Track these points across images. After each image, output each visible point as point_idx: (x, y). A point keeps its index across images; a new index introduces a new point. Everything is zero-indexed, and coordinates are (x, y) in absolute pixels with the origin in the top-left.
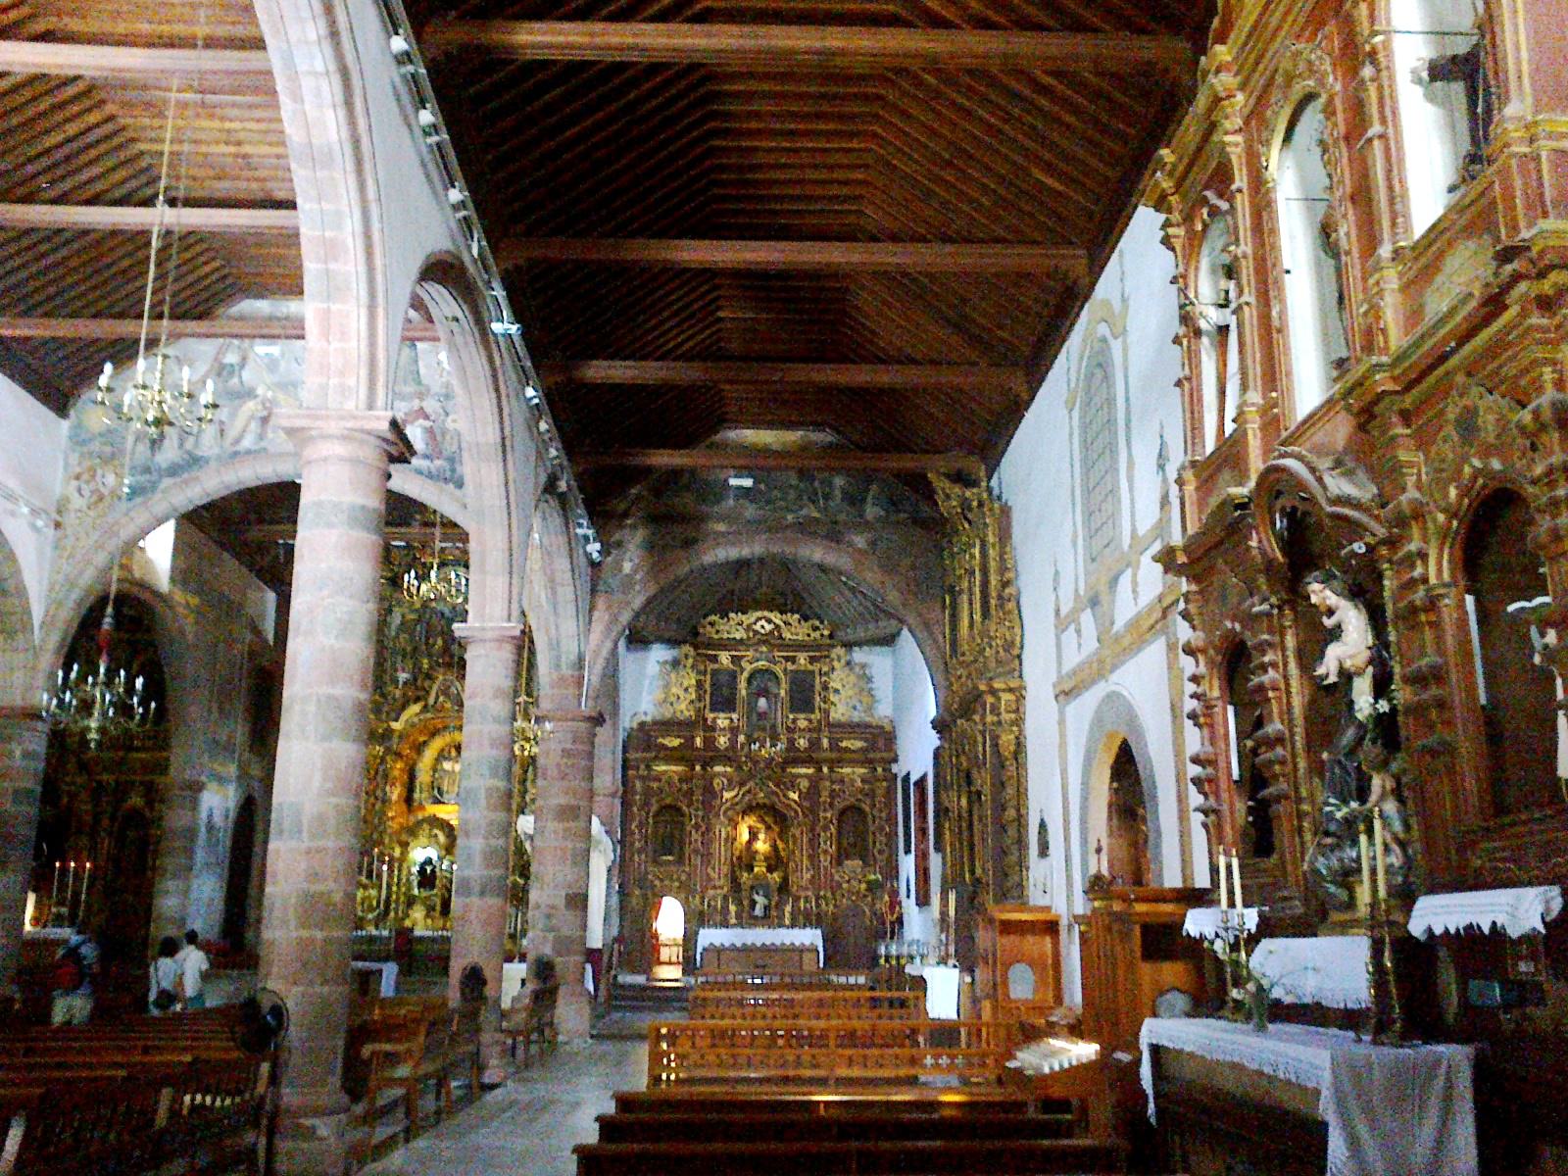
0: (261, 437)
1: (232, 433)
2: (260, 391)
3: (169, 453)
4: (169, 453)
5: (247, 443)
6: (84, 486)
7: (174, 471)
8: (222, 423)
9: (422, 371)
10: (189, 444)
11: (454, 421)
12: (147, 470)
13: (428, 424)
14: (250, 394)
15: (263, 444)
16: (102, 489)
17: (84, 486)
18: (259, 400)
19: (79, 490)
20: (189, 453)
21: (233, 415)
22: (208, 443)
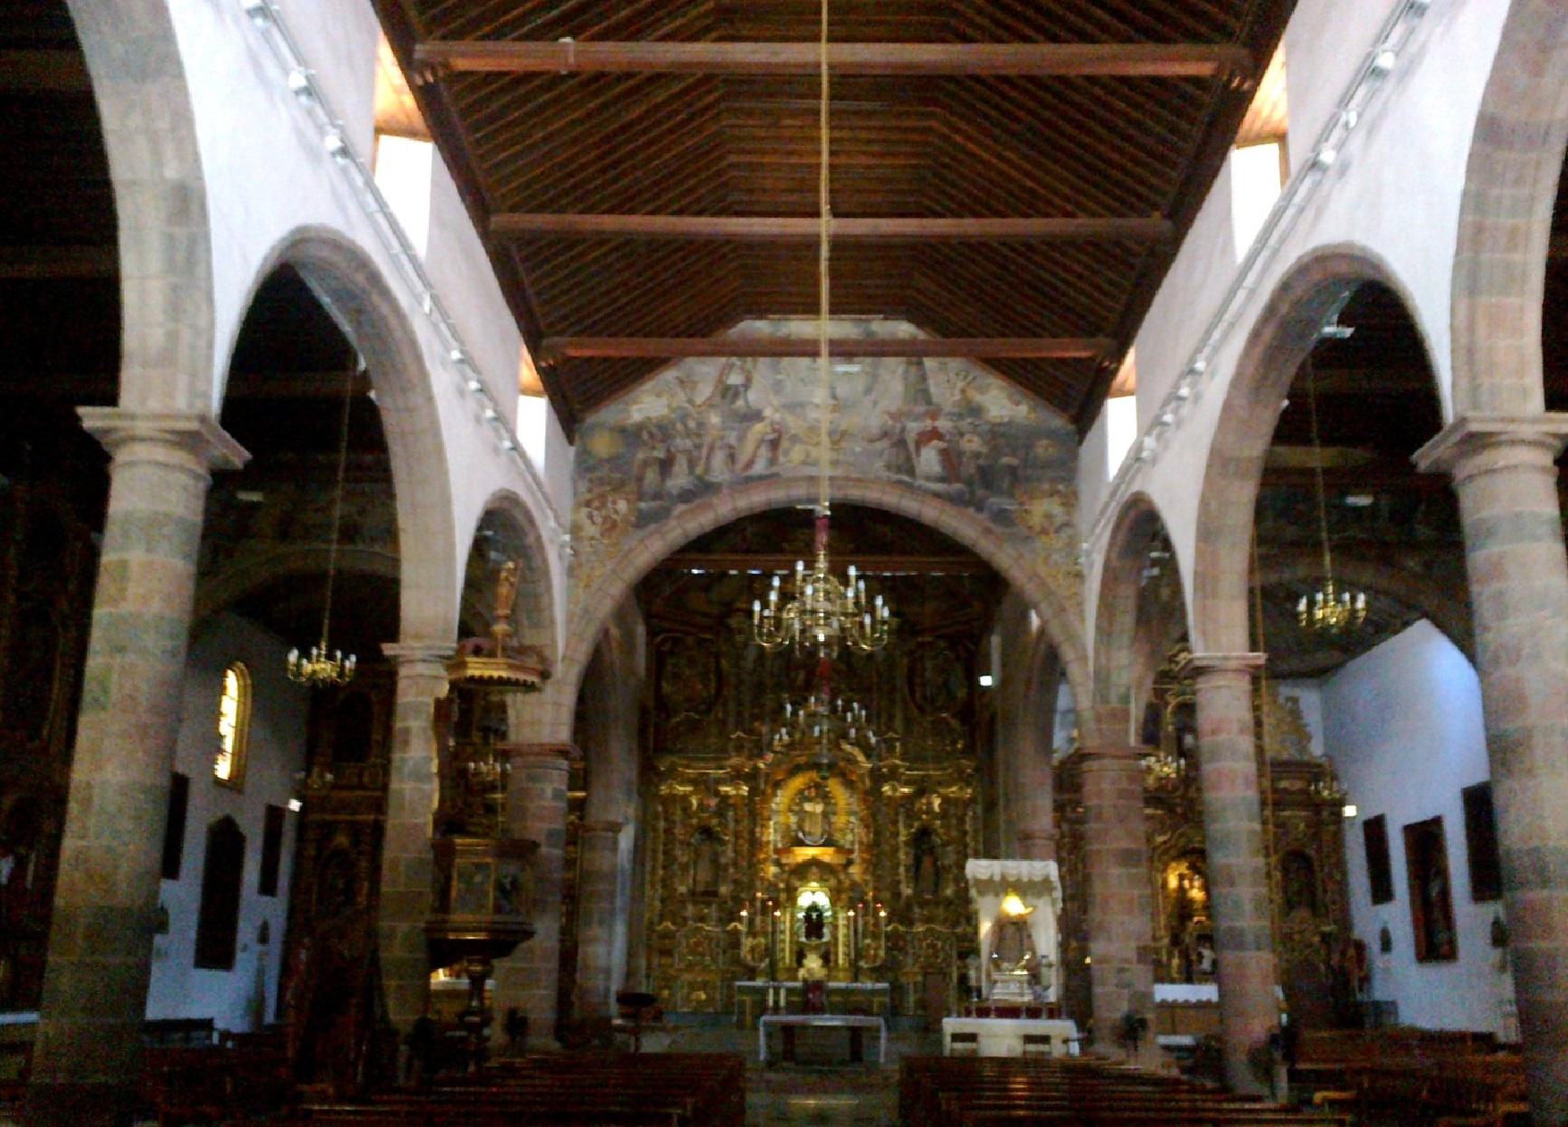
0: (773, 461)
1: (743, 458)
2: (767, 412)
3: (680, 479)
4: (680, 479)
5: (759, 468)
6: (595, 513)
7: (686, 496)
8: (731, 447)
9: (933, 390)
10: (699, 470)
11: (970, 441)
12: (657, 496)
13: (942, 445)
14: (756, 416)
15: (774, 469)
16: (614, 516)
17: (595, 513)
18: (767, 422)
19: (590, 517)
20: (700, 478)
21: (741, 439)
22: (719, 470)
